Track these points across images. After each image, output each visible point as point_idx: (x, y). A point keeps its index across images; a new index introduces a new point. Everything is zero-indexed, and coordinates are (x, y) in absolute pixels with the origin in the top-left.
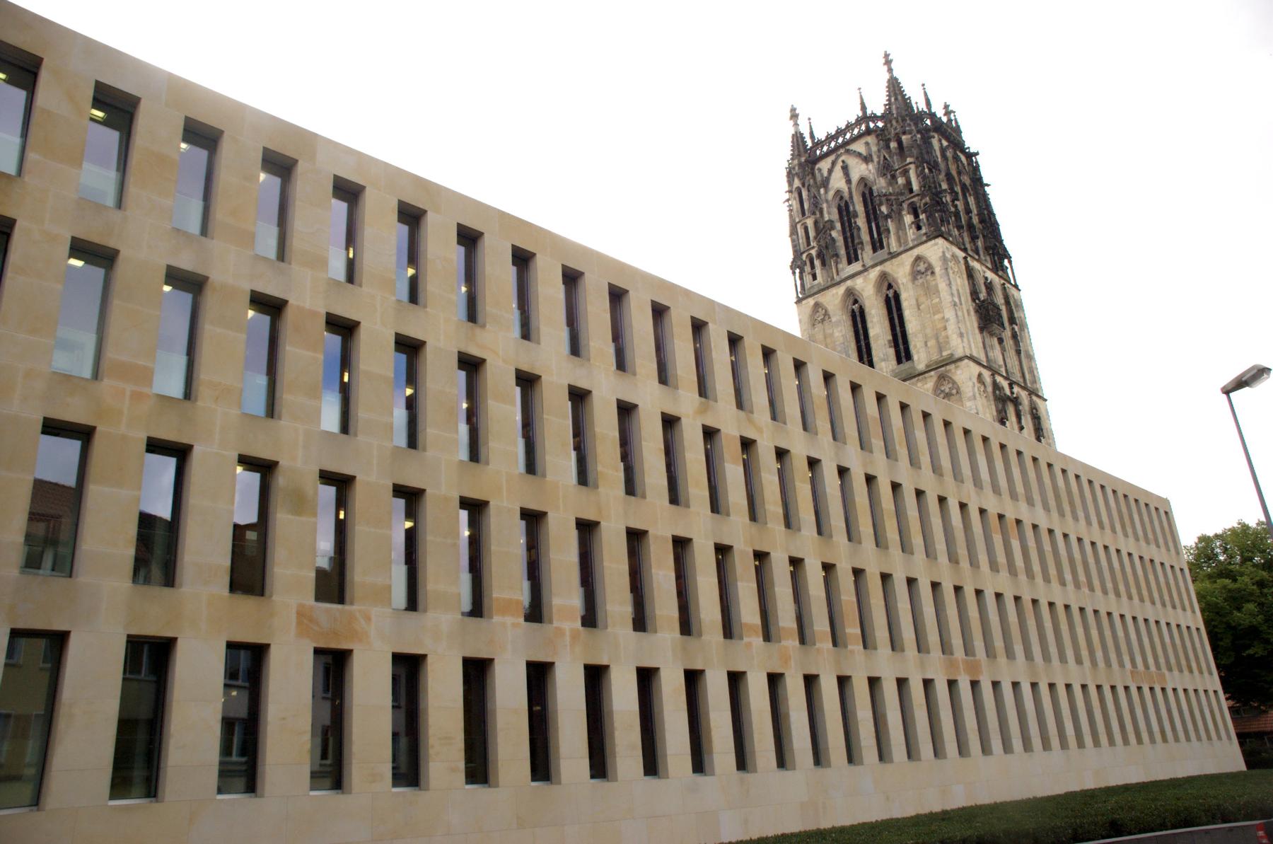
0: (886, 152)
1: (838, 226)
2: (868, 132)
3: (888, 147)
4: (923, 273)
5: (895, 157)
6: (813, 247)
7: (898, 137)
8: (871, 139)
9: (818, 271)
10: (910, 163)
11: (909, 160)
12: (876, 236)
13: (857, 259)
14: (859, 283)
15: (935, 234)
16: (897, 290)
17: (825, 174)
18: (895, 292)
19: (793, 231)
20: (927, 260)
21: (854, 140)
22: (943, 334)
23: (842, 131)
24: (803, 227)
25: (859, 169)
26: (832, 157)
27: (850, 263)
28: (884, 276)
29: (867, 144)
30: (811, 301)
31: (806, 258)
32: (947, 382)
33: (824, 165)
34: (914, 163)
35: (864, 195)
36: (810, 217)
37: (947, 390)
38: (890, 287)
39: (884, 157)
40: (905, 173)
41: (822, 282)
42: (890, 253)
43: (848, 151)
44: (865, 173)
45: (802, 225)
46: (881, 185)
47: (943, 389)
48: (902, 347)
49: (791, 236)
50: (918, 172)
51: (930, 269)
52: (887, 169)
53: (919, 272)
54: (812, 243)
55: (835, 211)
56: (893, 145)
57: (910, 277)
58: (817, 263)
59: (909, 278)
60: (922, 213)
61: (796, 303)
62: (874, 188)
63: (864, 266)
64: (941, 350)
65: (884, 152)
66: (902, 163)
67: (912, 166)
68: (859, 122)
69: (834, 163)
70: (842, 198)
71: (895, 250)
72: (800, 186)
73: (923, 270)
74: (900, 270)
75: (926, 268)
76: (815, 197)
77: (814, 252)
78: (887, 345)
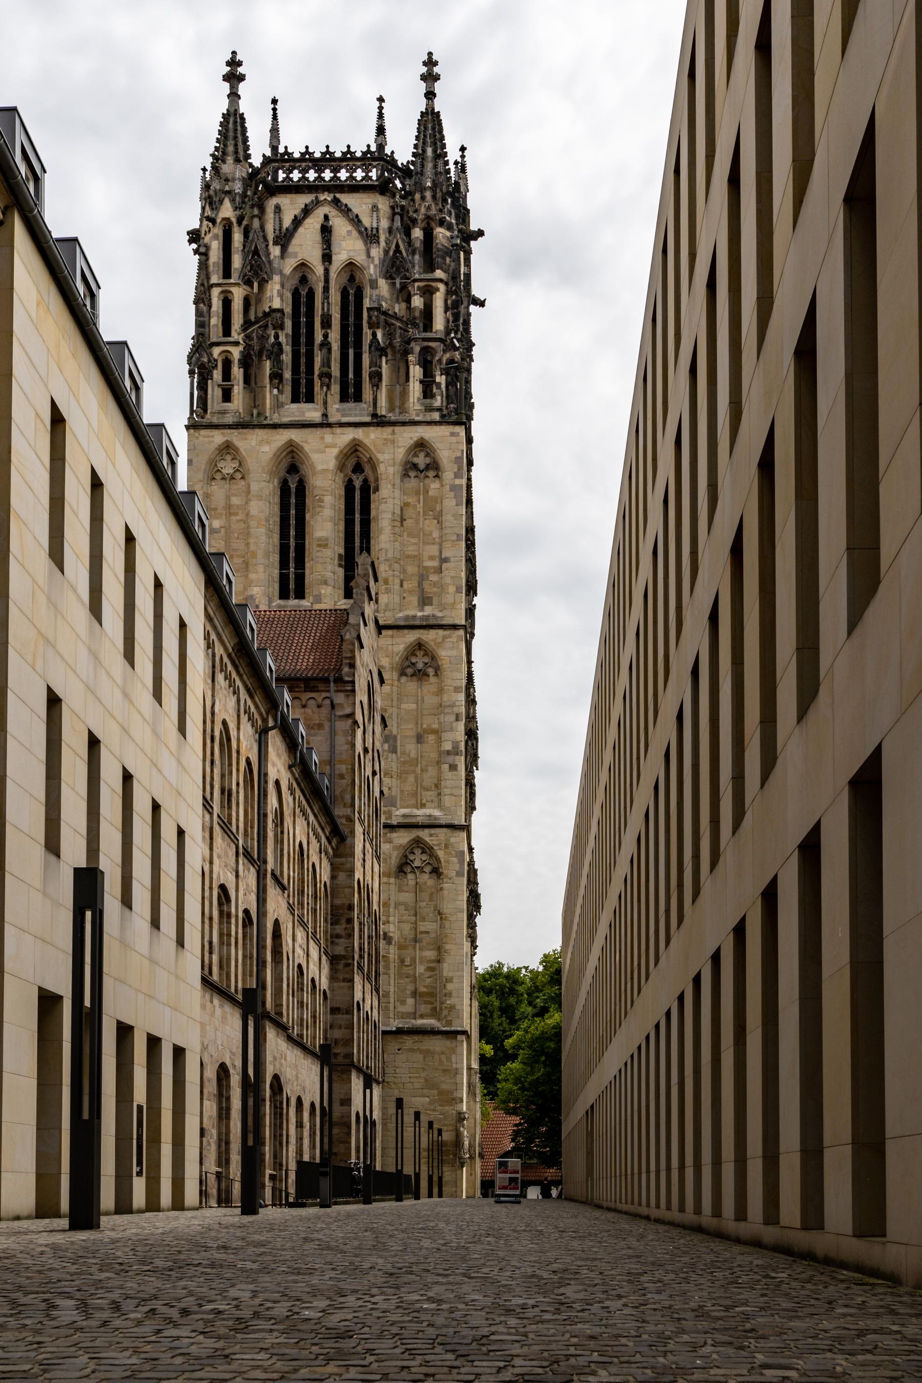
0: (403, 240)
1: (288, 323)
2: (383, 188)
3: (408, 233)
4: (420, 471)
5: (417, 257)
6: (236, 344)
7: (428, 224)
8: (384, 204)
9: (238, 390)
10: (441, 280)
11: (439, 274)
12: (351, 375)
13: (310, 399)
14: (308, 441)
15: (454, 418)
16: (371, 479)
17: (287, 222)
18: (366, 481)
19: (202, 298)
20: (434, 451)
21: (354, 188)
22: (434, 578)
23: (333, 159)
24: (222, 297)
26: (305, 199)
27: (295, 399)
28: (355, 448)
29: (375, 208)
30: (218, 437)
31: (219, 355)
32: (422, 653)
33: (291, 205)
34: (446, 284)
35: (344, 294)
36: (238, 284)
37: (420, 666)
38: (358, 468)
39: (397, 246)
40: (428, 292)
41: (241, 411)
42: (374, 415)
43: (336, 202)
44: (360, 259)
45: (222, 292)
47: (414, 660)
49: (196, 302)
50: (449, 302)
51: (434, 467)
52: (398, 270)
53: (415, 466)
54: (234, 333)
55: (288, 296)
56: (417, 233)
57: (401, 468)
58: (237, 372)
59: (399, 469)
60: (441, 374)
61: (188, 428)
62: (368, 291)
63: (325, 415)
65: (399, 238)
66: (425, 272)
67: (442, 287)
69: (307, 211)
70: (304, 280)
71: (384, 413)
72: (234, 220)
73: (422, 466)
75: (428, 465)
76: (256, 252)
77: (236, 353)
78: (336, 562)
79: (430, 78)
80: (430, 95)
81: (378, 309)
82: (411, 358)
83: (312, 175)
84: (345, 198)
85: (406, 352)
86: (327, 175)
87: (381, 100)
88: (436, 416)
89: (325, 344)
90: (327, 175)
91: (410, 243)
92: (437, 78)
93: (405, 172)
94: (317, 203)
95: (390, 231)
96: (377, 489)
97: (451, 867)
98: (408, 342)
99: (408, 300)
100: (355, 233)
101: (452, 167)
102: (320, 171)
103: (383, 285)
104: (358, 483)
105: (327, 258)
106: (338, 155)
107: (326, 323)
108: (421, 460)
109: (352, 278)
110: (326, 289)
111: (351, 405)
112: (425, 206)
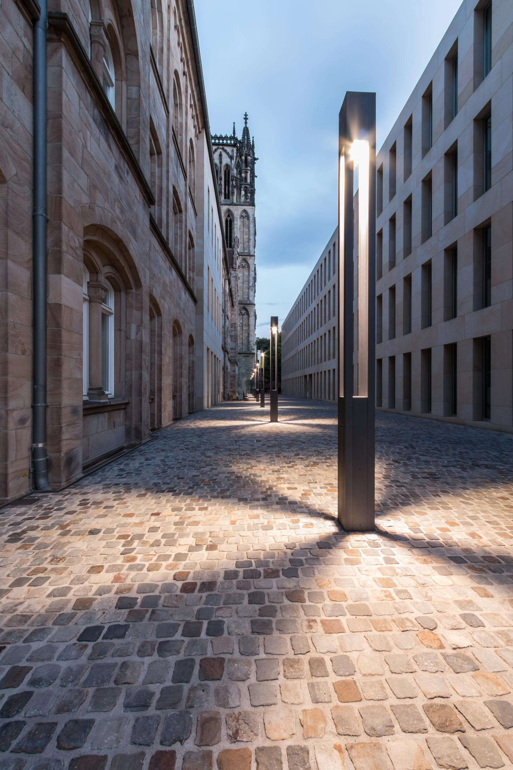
2: (234, 145)
3: (241, 157)
11: (249, 168)
21: (227, 145)
22: (247, 244)
23: (222, 137)
25: (226, 160)
28: (229, 211)
29: (233, 151)
35: (225, 172)
40: (246, 173)
43: (223, 149)
44: (229, 163)
46: (235, 172)
48: (229, 242)
51: (248, 217)
56: (243, 158)
62: (231, 172)
64: (244, 249)
67: (249, 172)
68: (231, 138)
74: (237, 211)
79: (246, 119)
80: (246, 123)
81: (234, 176)
82: (242, 189)
83: (217, 141)
84: (226, 148)
85: (240, 188)
86: (221, 141)
87: (234, 123)
88: (248, 204)
89: (221, 184)
90: (221, 141)
91: (241, 160)
92: (247, 119)
93: (240, 142)
94: (218, 148)
95: (237, 157)
96: (234, 221)
97: (252, 314)
98: (241, 185)
99: (241, 174)
100: (228, 157)
101: (251, 141)
102: (219, 140)
103: (235, 171)
104: (229, 219)
105: (221, 162)
106: (224, 136)
107: (221, 179)
108: (244, 215)
109: (227, 168)
110: (221, 170)
111: (227, 200)
112: (245, 150)
